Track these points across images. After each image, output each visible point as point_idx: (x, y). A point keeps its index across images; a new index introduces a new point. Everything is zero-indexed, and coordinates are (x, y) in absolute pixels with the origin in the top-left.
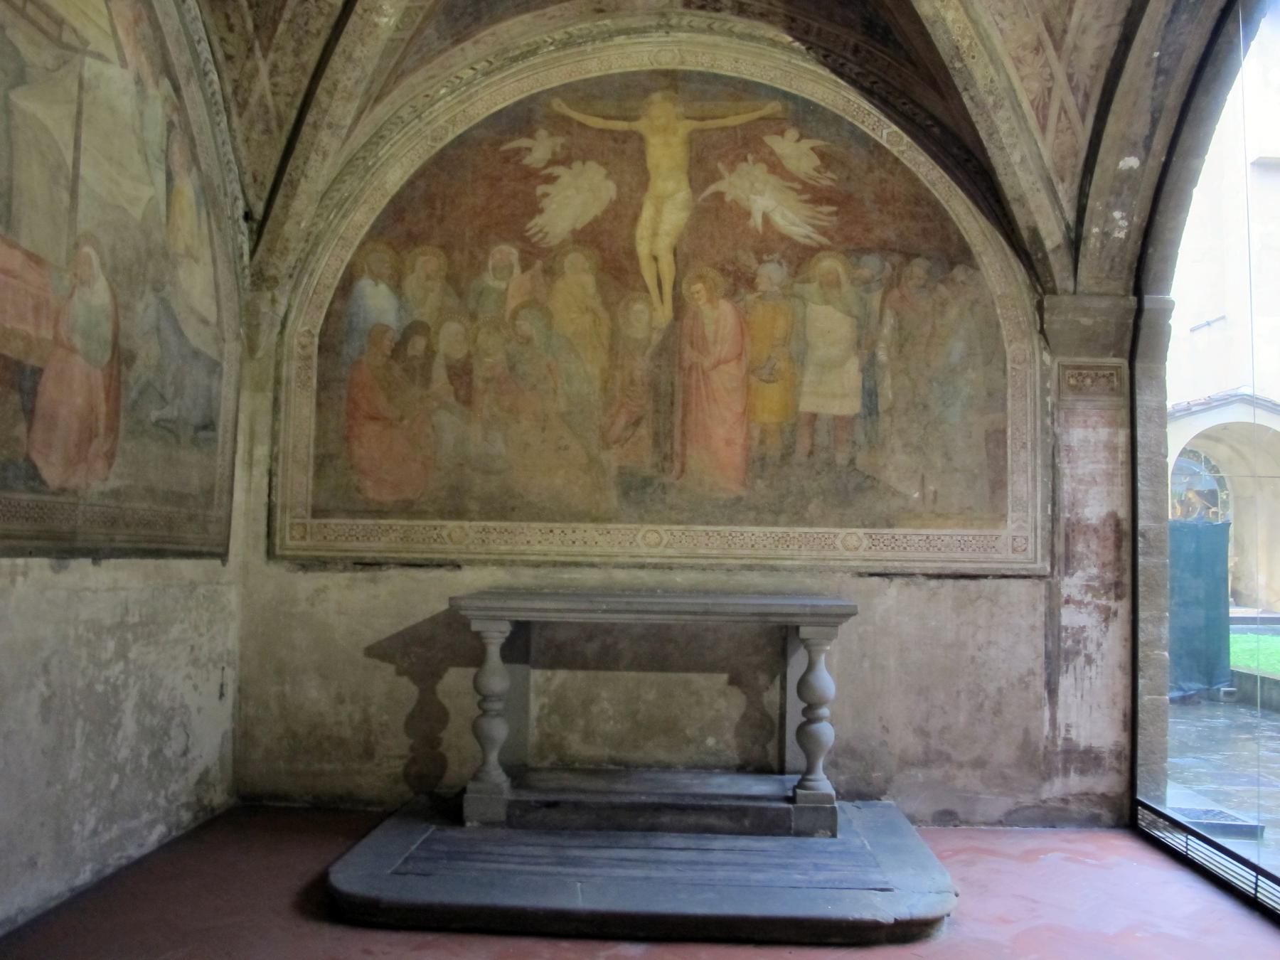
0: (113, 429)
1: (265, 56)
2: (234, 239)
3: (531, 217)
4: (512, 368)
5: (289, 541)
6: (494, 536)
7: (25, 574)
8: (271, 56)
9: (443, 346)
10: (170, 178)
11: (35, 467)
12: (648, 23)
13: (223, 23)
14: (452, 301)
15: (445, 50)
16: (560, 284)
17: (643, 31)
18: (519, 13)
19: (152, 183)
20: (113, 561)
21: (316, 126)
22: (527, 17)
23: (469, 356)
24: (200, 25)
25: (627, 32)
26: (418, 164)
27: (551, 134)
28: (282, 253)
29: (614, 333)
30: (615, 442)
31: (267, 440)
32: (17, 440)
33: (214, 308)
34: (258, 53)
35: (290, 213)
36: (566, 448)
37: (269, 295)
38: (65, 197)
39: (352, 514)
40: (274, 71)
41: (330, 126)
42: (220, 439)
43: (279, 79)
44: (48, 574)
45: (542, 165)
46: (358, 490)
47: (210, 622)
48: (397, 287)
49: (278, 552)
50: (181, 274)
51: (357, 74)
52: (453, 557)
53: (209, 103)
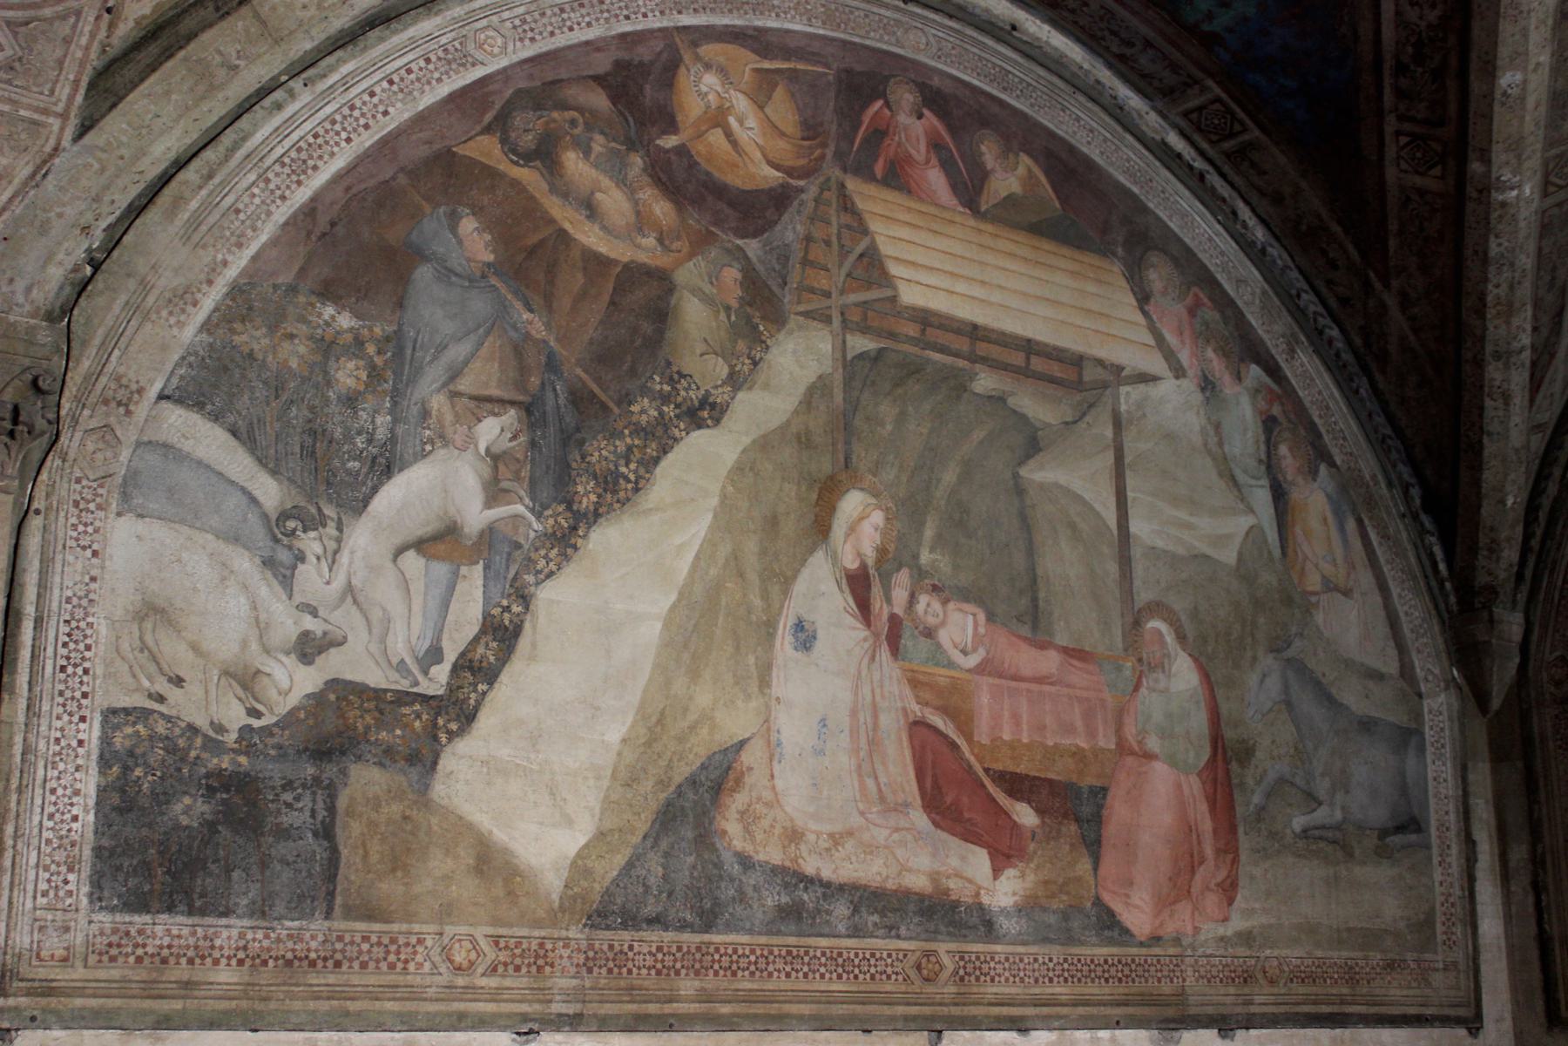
0: (1228, 848)
1: (1387, 286)
8: (1395, 283)
10: (1279, 494)
19: (1252, 511)
24: (1295, 274)
32: (1079, 880)
33: (1392, 652)
34: (1378, 285)
35: (1483, 491)
38: (1113, 568)
40: (1405, 302)
41: (1497, 356)
42: (1434, 841)
50: (1319, 618)
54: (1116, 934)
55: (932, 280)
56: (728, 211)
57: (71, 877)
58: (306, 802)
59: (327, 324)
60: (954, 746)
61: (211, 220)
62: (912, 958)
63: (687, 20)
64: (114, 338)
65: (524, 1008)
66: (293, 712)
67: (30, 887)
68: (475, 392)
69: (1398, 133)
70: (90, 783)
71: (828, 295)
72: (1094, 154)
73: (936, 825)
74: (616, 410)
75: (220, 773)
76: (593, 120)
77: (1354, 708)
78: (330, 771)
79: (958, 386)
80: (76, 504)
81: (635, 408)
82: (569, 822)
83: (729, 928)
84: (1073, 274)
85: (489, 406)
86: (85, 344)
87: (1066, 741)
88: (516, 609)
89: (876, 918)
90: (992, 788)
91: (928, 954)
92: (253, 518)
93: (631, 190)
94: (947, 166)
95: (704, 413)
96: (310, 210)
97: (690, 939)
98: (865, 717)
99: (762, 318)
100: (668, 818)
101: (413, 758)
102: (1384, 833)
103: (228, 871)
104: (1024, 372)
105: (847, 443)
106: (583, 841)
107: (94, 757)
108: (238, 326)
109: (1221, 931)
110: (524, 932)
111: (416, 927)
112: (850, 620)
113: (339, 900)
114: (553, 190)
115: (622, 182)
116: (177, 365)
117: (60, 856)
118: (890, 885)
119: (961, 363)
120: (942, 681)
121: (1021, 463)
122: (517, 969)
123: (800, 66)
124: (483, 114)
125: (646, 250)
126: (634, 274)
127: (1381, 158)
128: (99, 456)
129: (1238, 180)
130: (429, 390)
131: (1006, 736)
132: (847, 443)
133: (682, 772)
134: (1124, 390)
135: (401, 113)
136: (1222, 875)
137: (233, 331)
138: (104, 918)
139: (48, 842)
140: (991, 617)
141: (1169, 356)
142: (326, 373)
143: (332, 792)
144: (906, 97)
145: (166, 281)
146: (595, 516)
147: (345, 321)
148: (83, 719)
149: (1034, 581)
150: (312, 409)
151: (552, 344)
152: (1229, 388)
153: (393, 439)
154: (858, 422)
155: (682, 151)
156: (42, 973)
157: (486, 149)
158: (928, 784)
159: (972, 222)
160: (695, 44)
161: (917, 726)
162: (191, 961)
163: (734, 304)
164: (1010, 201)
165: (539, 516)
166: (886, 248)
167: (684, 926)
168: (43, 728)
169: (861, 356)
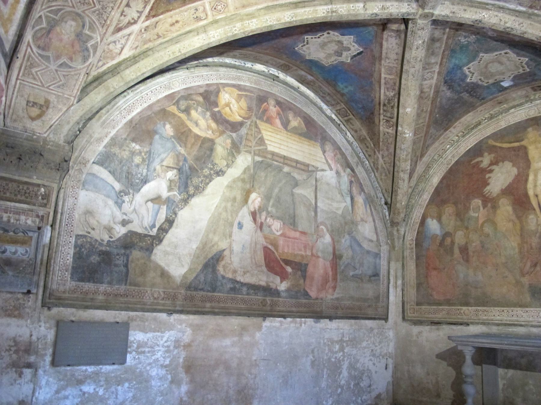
0: (335, 279)
1: (379, 153)
2: (382, 212)
3: (485, 187)
4: (483, 247)
5: (409, 314)
6: (481, 313)
7: (305, 323)
8: (381, 152)
9: (457, 241)
10: (352, 199)
11: (307, 292)
12: (521, 102)
13: (365, 146)
14: (459, 223)
15: (443, 134)
16: (498, 212)
17: (521, 104)
18: (467, 113)
19: (345, 202)
20: (337, 320)
21: (398, 172)
22: (470, 114)
23: (467, 243)
24: (359, 148)
25: (514, 107)
26: (443, 174)
27: (489, 154)
28: (398, 214)
29: (522, 229)
30: (527, 274)
31: (401, 279)
33: (375, 236)
34: (377, 152)
36: (506, 277)
37: (396, 228)
39: (429, 304)
40: (383, 157)
41: (402, 171)
42: (381, 279)
43: (385, 159)
44: (313, 323)
45: (487, 166)
46: (431, 295)
47: (380, 342)
48: (439, 220)
49: (406, 318)
50: (359, 227)
51: (405, 153)
52: (466, 321)
53: (366, 170)
54: (308, 297)
55: (276, 145)
56: (229, 126)
57: (66, 273)
58: (122, 258)
59: (133, 148)
60: (273, 253)
61: (108, 122)
62: (260, 301)
63: (223, 81)
64: (83, 148)
65: (170, 308)
66: (120, 238)
67: (57, 275)
68: (167, 165)
69: (383, 119)
70: (72, 252)
71: (251, 147)
72: (315, 119)
73: (268, 270)
74: (200, 171)
75: (101, 251)
76: (198, 103)
77: (366, 248)
78: (128, 252)
79: (280, 170)
80: (72, 187)
81: (204, 171)
82: (183, 266)
83: (219, 292)
84: (309, 145)
85: (169, 169)
86: (76, 149)
87: (300, 253)
88: (174, 216)
89: (253, 291)
90: (281, 263)
91: (264, 300)
92: (113, 192)
93: (207, 120)
94: (281, 119)
95: (220, 173)
96: (131, 121)
97: (210, 294)
98: (253, 245)
99: (236, 152)
100: (206, 266)
101: (147, 250)
102: (370, 277)
103: (103, 273)
104: (296, 167)
105: (253, 181)
106: (186, 270)
107: (73, 246)
108: (112, 147)
109: (332, 297)
110: (171, 291)
111: (146, 289)
112: (251, 223)
113: (128, 281)
114: (188, 119)
115: (204, 118)
116: (98, 155)
117: (64, 268)
118: (257, 284)
119: (281, 165)
120: (272, 238)
121: (294, 188)
122: (169, 299)
123: (248, 94)
124: (173, 100)
125: (209, 134)
126: (205, 140)
127: (379, 124)
128: (78, 176)
129: (347, 127)
130: (156, 165)
131: (286, 251)
132: (253, 181)
133: (210, 256)
134: (318, 173)
135: (154, 99)
136: (333, 285)
137: (111, 148)
138: (74, 283)
139: (61, 265)
140: (284, 224)
141: (329, 165)
142: (132, 159)
143: (128, 256)
144: (272, 102)
145: (96, 136)
146: (193, 196)
147: (138, 147)
148: (71, 237)
149: (294, 216)
150: (128, 167)
151: (186, 155)
152: (342, 174)
153: (147, 175)
154: (256, 177)
155: (219, 112)
156: (59, 295)
157: (173, 109)
158: (267, 261)
159: (285, 132)
160: (224, 87)
161: (265, 249)
162: (93, 294)
163: (229, 148)
164: (295, 128)
165: (180, 195)
166: (265, 137)
167: (208, 291)
168: (62, 239)
169: (258, 162)
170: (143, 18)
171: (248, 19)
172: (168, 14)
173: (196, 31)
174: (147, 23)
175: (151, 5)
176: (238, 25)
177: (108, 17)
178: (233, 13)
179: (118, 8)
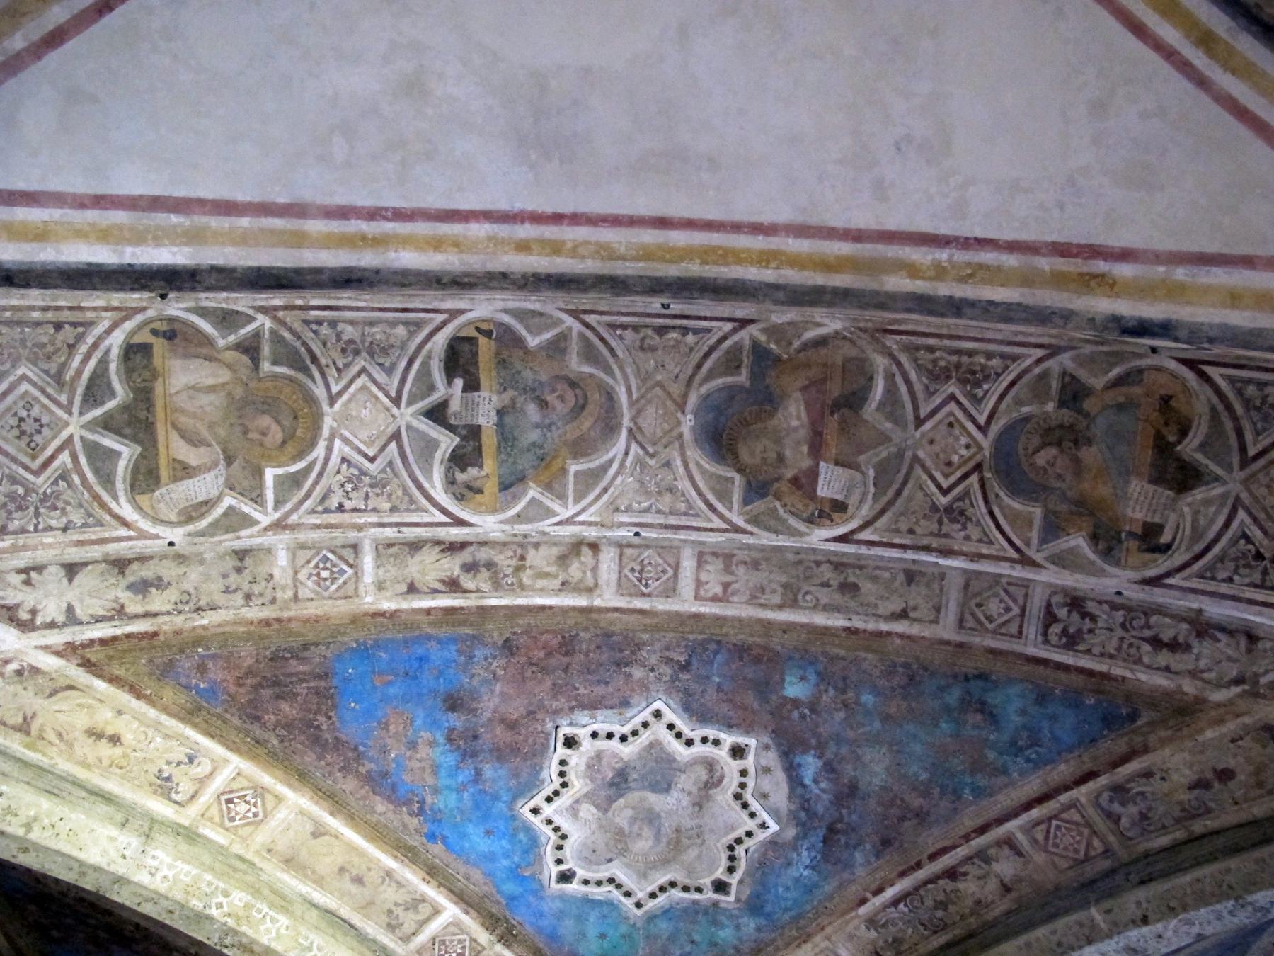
170: (57, 638)
171: (272, 906)
172: (125, 698)
173: (127, 816)
174: (49, 662)
175: (118, 632)
176: (239, 898)
177: (23, 531)
178: (249, 856)
179: (81, 543)
